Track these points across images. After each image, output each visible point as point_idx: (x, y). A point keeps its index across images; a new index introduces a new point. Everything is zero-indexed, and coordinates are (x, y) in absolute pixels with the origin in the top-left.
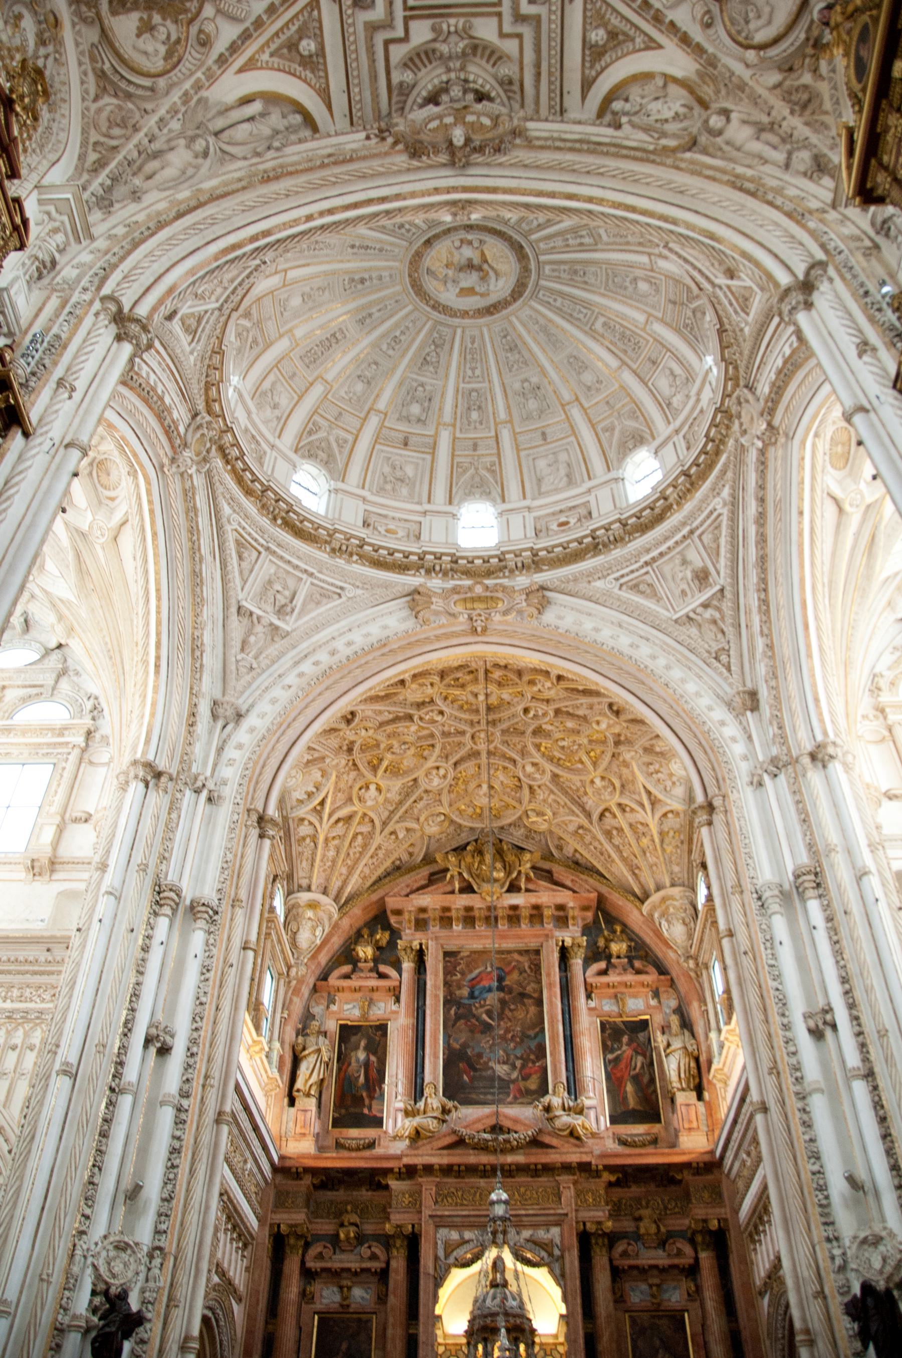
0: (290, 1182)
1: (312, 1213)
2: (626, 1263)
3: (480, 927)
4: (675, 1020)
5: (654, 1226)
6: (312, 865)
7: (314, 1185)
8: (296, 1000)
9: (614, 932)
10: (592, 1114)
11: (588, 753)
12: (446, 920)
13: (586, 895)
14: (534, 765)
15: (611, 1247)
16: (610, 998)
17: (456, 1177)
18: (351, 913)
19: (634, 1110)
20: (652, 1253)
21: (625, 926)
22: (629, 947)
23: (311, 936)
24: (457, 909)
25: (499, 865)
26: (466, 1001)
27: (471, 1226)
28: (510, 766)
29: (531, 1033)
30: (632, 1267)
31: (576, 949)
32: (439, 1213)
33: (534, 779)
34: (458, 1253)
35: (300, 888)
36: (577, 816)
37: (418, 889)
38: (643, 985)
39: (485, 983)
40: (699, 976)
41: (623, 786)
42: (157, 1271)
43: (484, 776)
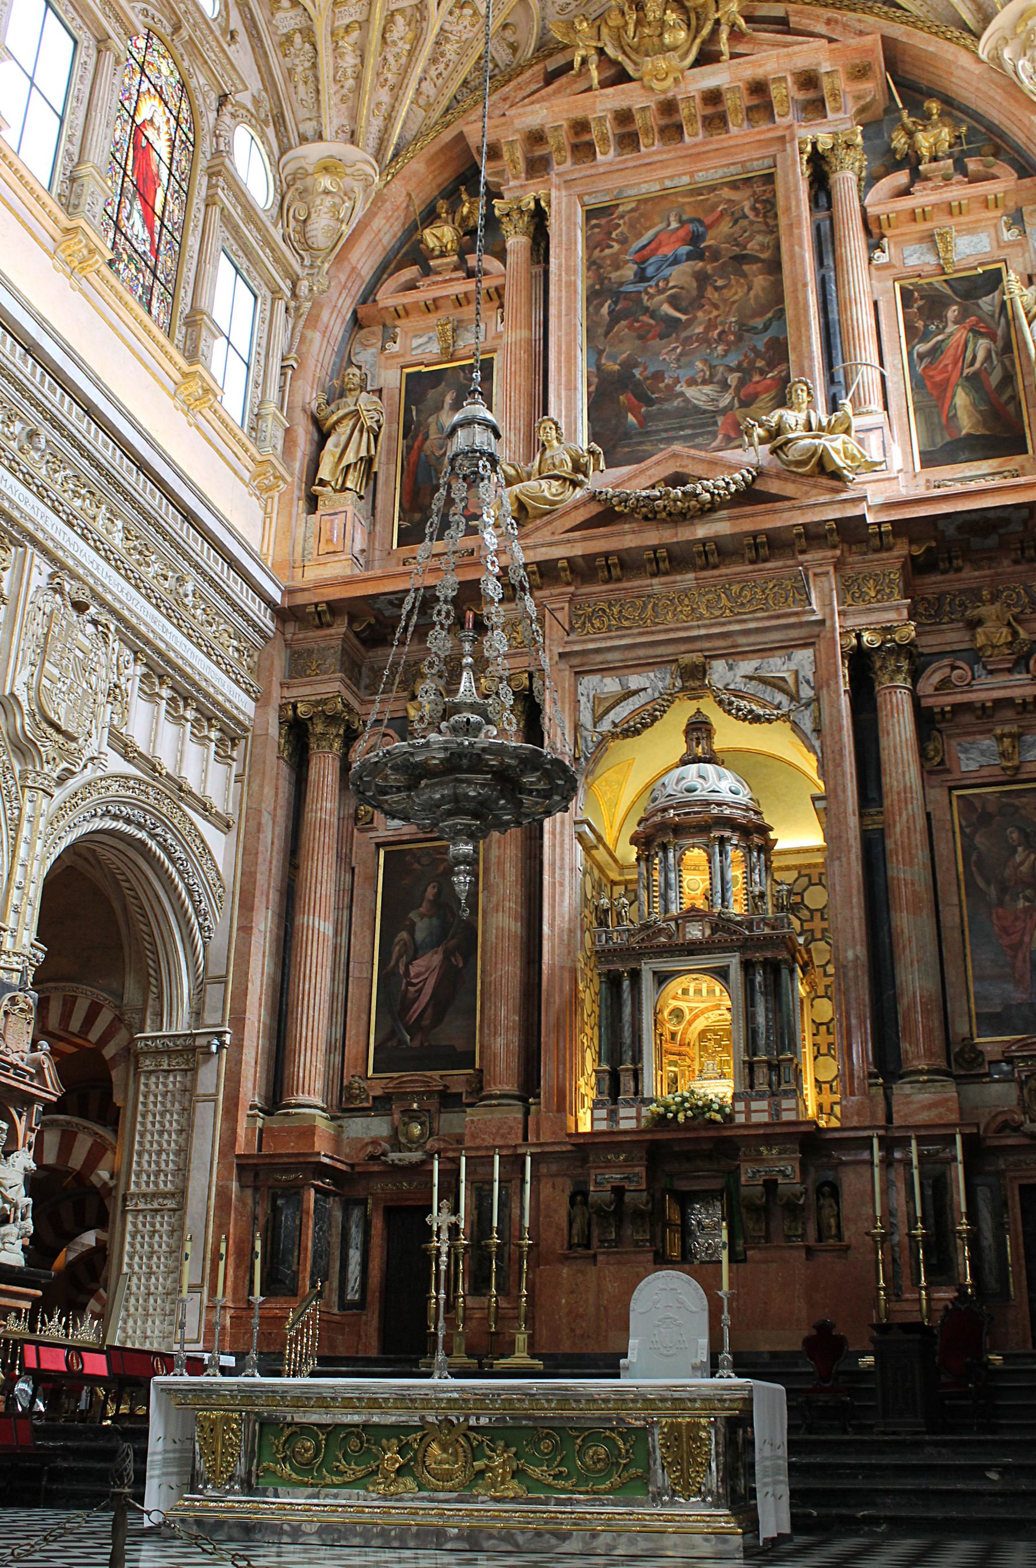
0: (311, 634)
1: (366, 688)
2: (947, 700)
3: (651, 148)
5: (1005, 630)
6: (318, 91)
7: (357, 634)
8: (317, 336)
9: (928, 116)
10: (874, 440)
12: (584, 150)
13: (854, 41)
15: (915, 675)
16: (921, 240)
17: (607, 582)
18: (405, 172)
19: (969, 436)
20: (1001, 679)
21: (948, 102)
23: (333, 223)
24: (601, 120)
25: (671, 17)
26: (631, 288)
29: (759, 323)
30: (959, 708)
31: (841, 152)
32: (577, 648)
34: (620, 713)
35: (303, 139)
37: (524, 98)
39: (667, 251)
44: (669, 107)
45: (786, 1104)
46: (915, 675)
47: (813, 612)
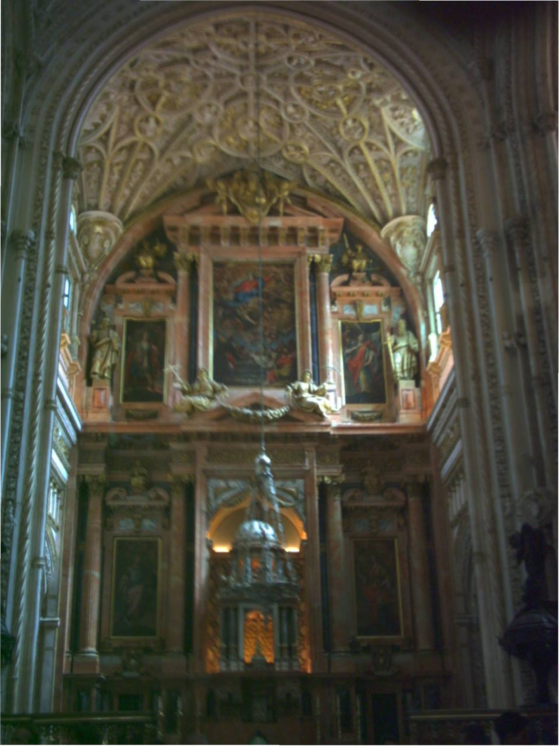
2: (353, 505)
3: (245, 245)
4: (402, 324)
9: (355, 250)
10: (332, 395)
11: (343, 98)
13: (334, 220)
14: (295, 106)
19: (364, 393)
22: (368, 264)
27: (235, 478)
28: (274, 106)
30: (356, 508)
31: (324, 264)
33: (294, 119)
36: (330, 152)
38: (377, 294)
39: (248, 290)
40: (424, 291)
41: (371, 127)
42: (11, 516)
43: (252, 113)
44: (255, 229)
45: (295, 664)
46: (342, 494)
47: (306, 466)
